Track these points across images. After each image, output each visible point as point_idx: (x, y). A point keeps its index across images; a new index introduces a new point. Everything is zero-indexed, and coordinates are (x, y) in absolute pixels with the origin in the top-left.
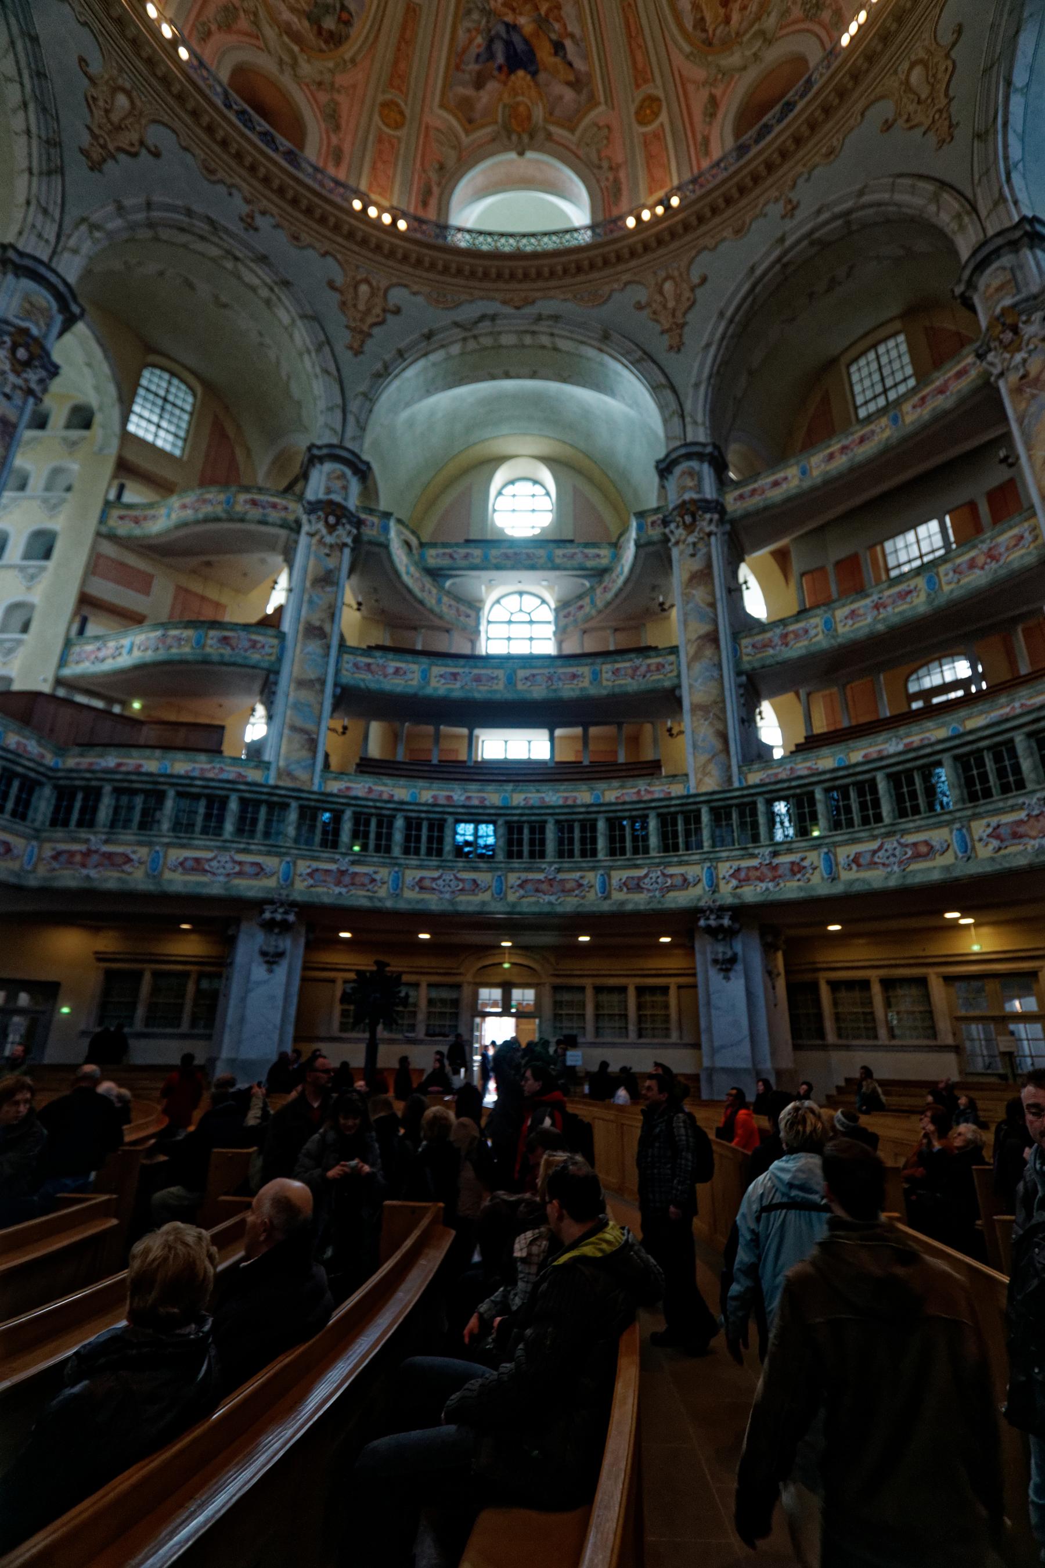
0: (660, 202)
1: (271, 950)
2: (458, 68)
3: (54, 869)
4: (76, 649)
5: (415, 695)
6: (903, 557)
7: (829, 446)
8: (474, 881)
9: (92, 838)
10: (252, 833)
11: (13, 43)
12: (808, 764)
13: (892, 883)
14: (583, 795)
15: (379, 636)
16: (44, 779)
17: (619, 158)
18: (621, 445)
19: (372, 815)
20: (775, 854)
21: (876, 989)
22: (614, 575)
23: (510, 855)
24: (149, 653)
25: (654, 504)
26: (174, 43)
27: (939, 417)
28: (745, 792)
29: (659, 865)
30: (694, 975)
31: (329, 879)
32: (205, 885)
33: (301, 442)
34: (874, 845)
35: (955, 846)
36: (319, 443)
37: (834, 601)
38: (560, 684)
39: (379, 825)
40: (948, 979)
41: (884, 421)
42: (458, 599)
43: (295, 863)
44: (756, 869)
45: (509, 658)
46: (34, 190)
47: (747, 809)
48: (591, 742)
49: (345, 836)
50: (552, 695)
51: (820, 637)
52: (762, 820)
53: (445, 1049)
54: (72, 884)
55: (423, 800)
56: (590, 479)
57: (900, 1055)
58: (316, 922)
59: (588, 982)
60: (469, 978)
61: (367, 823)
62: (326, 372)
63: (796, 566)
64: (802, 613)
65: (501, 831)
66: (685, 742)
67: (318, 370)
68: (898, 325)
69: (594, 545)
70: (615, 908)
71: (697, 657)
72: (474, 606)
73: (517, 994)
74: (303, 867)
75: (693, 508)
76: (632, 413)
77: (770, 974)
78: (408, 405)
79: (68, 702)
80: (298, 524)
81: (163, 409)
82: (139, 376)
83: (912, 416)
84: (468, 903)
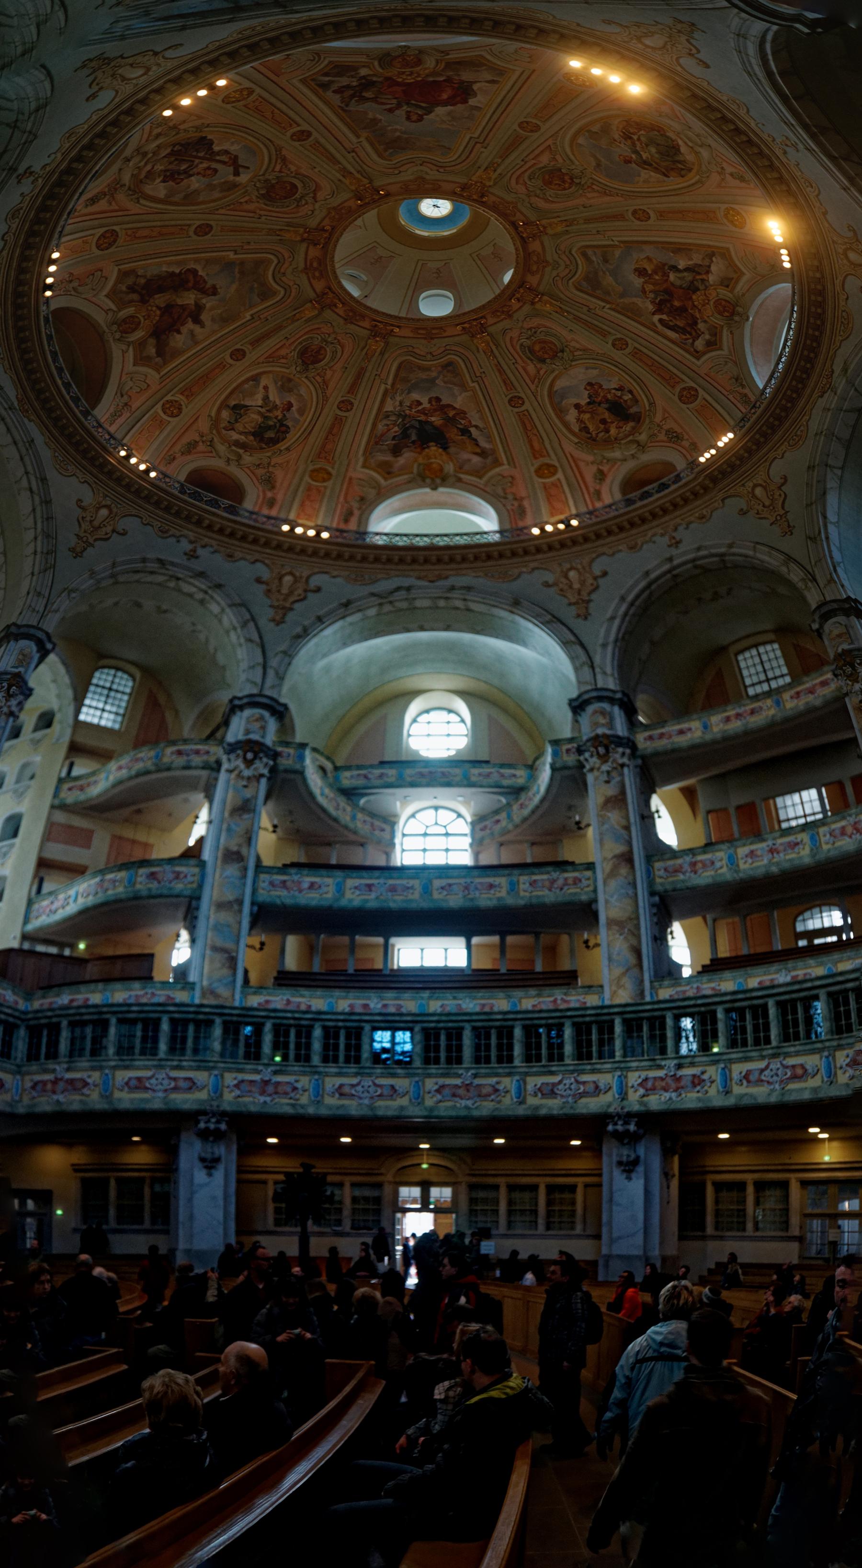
0: (562, 522)
1: (209, 1156)
2: (377, 443)
3: (34, 1098)
4: (36, 907)
5: (330, 908)
6: (791, 814)
7: (725, 711)
8: (392, 1087)
9: (57, 1067)
10: (183, 1050)
11: (34, 510)
12: (713, 985)
13: (773, 1099)
14: (501, 1003)
15: (295, 854)
16: (19, 1022)
17: (523, 494)
18: (534, 685)
19: (290, 1026)
20: (679, 1066)
21: (750, 1189)
22: (530, 794)
23: (427, 1061)
24: (91, 898)
25: (567, 733)
26: (147, 471)
27: (811, 710)
28: (656, 1006)
29: (572, 1072)
30: (600, 1175)
31: (254, 1089)
32: (147, 1101)
33: (224, 697)
34: (762, 1064)
35: (823, 1071)
36: (240, 695)
37: (737, 840)
38: (477, 893)
39: (298, 1035)
40: (804, 1183)
41: (769, 702)
42: (373, 815)
43: (222, 1076)
44: (662, 1079)
45: (424, 868)
46: (33, 584)
47: (657, 1023)
48: (508, 950)
49: (267, 1048)
50: (468, 904)
51: (724, 870)
52: (670, 1034)
53: (369, 1240)
54: (48, 1108)
55: (340, 1009)
56: (505, 710)
57: (760, 1244)
58: (245, 1129)
59: (502, 1181)
60: (389, 1177)
61: (287, 1035)
62: (250, 640)
63: (703, 804)
64: (709, 846)
65: (418, 1037)
66: (600, 955)
67: (242, 640)
68: (772, 636)
69: (510, 766)
70: (529, 1113)
71: (612, 874)
72: (389, 821)
73: (435, 1192)
74: (230, 1079)
75: (605, 742)
76: (545, 660)
77: (666, 1175)
78: (325, 655)
79: (32, 953)
80: (219, 763)
81: (108, 696)
82: (91, 676)
83: (791, 704)
84: (387, 1107)
